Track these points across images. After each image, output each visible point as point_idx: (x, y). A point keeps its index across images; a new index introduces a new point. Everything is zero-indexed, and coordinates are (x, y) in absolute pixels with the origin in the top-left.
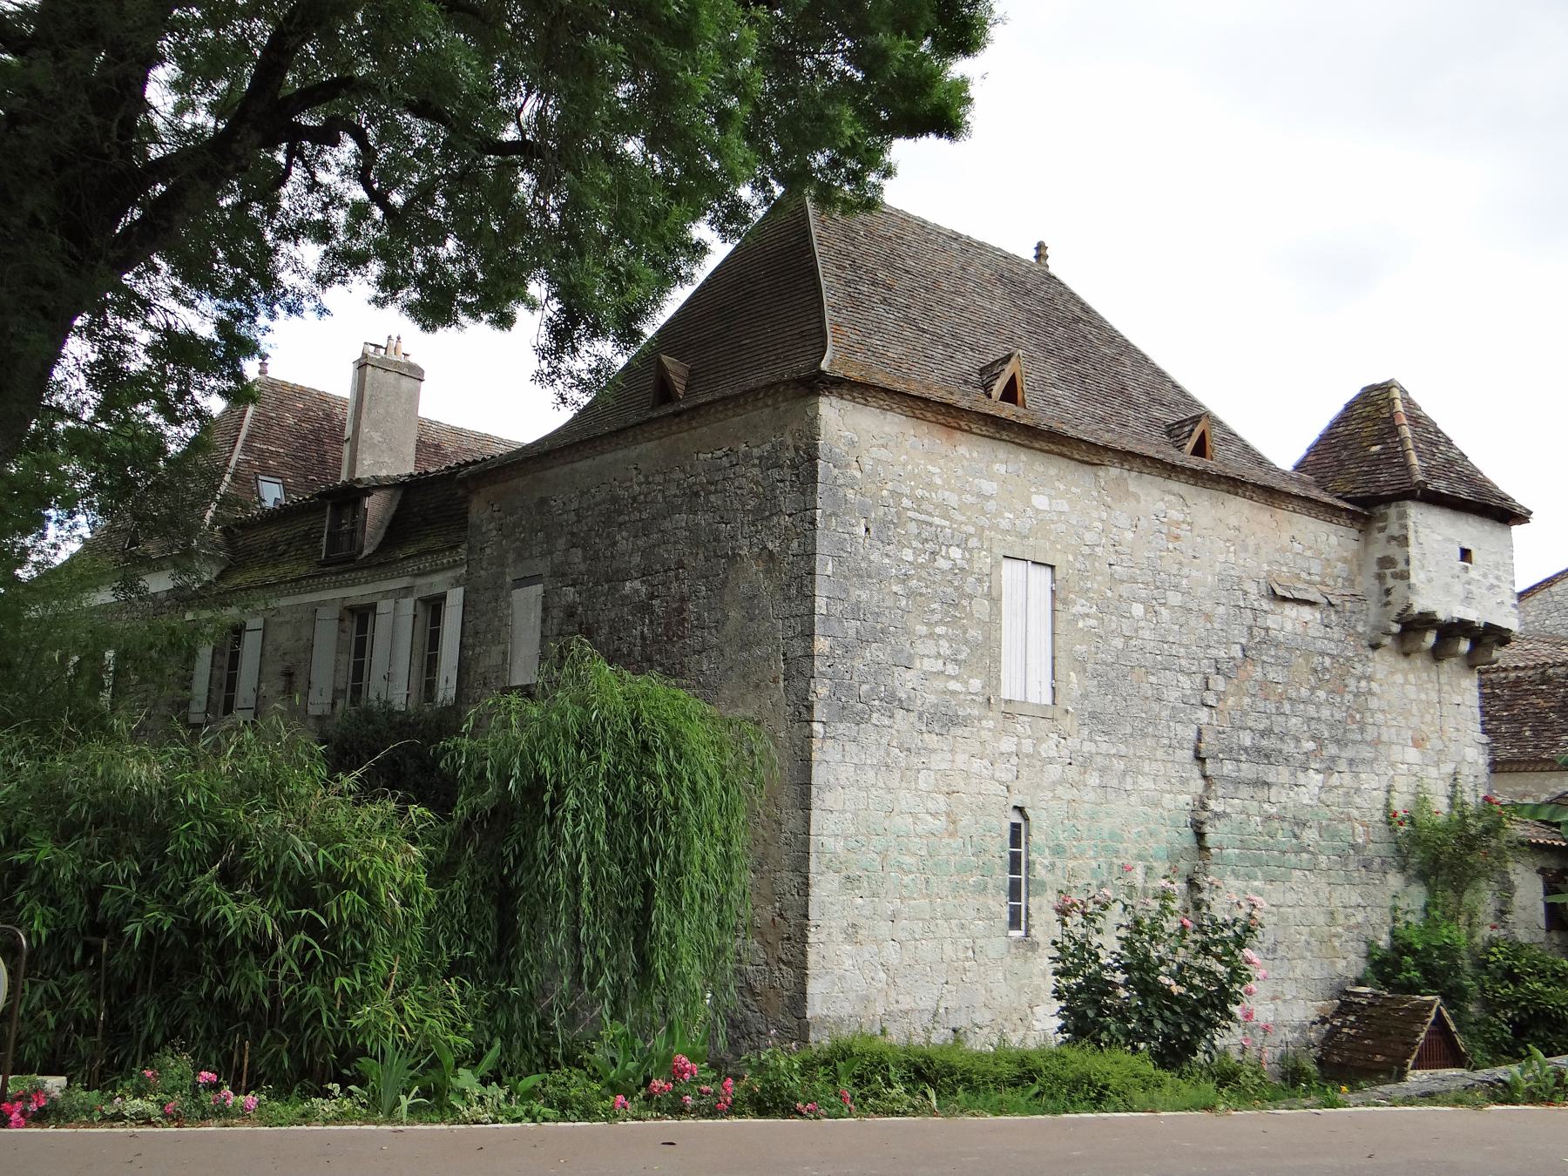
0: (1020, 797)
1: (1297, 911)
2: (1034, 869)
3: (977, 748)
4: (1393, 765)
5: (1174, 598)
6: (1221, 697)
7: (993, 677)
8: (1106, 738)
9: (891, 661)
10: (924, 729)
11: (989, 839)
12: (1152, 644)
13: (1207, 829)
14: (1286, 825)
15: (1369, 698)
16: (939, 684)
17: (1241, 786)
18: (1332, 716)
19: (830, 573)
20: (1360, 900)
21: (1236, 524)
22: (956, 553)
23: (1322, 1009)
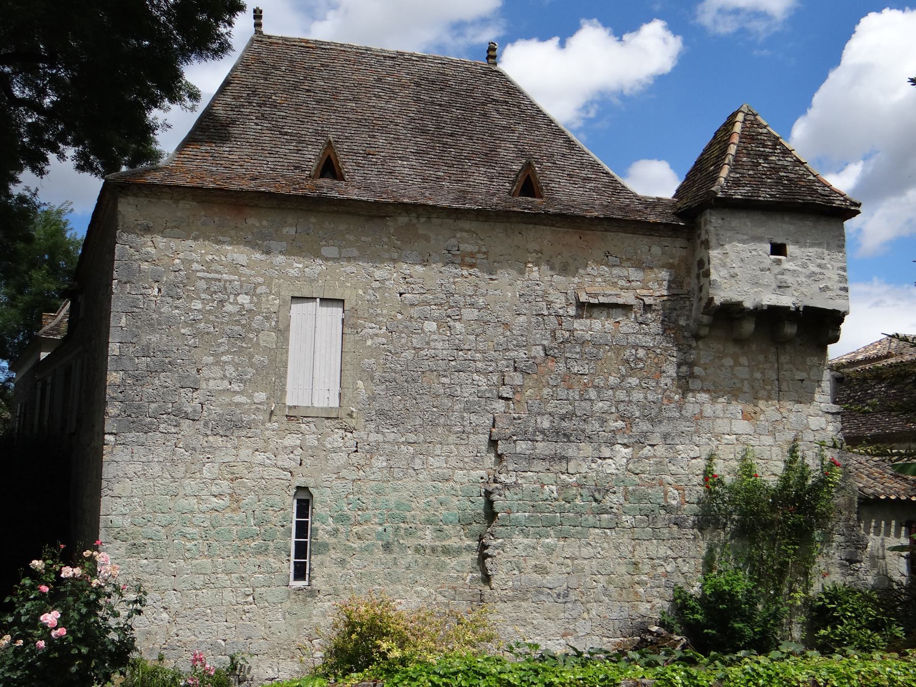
0: (303, 479)
1: (594, 562)
2: (317, 534)
3: (261, 444)
4: (718, 436)
5: (470, 314)
6: (515, 389)
7: (278, 389)
8: (395, 430)
9: (178, 385)
10: (209, 432)
11: (271, 513)
12: (445, 352)
13: (495, 497)
14: (585, 492)
15: (690, 381)
16: (226, 399)
17: (535, 462)
18: (646, 398)
19: (123, 325)
20: (669, 552)
21: (538, 248)
22: (244, 299)
23: (619, 644)
